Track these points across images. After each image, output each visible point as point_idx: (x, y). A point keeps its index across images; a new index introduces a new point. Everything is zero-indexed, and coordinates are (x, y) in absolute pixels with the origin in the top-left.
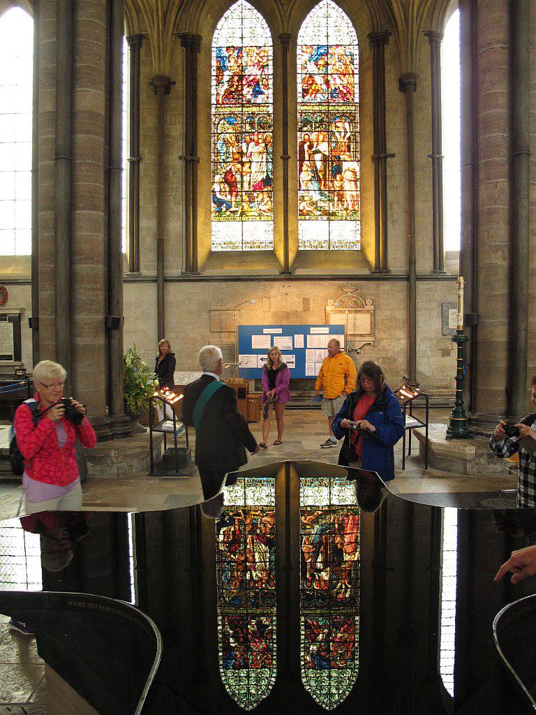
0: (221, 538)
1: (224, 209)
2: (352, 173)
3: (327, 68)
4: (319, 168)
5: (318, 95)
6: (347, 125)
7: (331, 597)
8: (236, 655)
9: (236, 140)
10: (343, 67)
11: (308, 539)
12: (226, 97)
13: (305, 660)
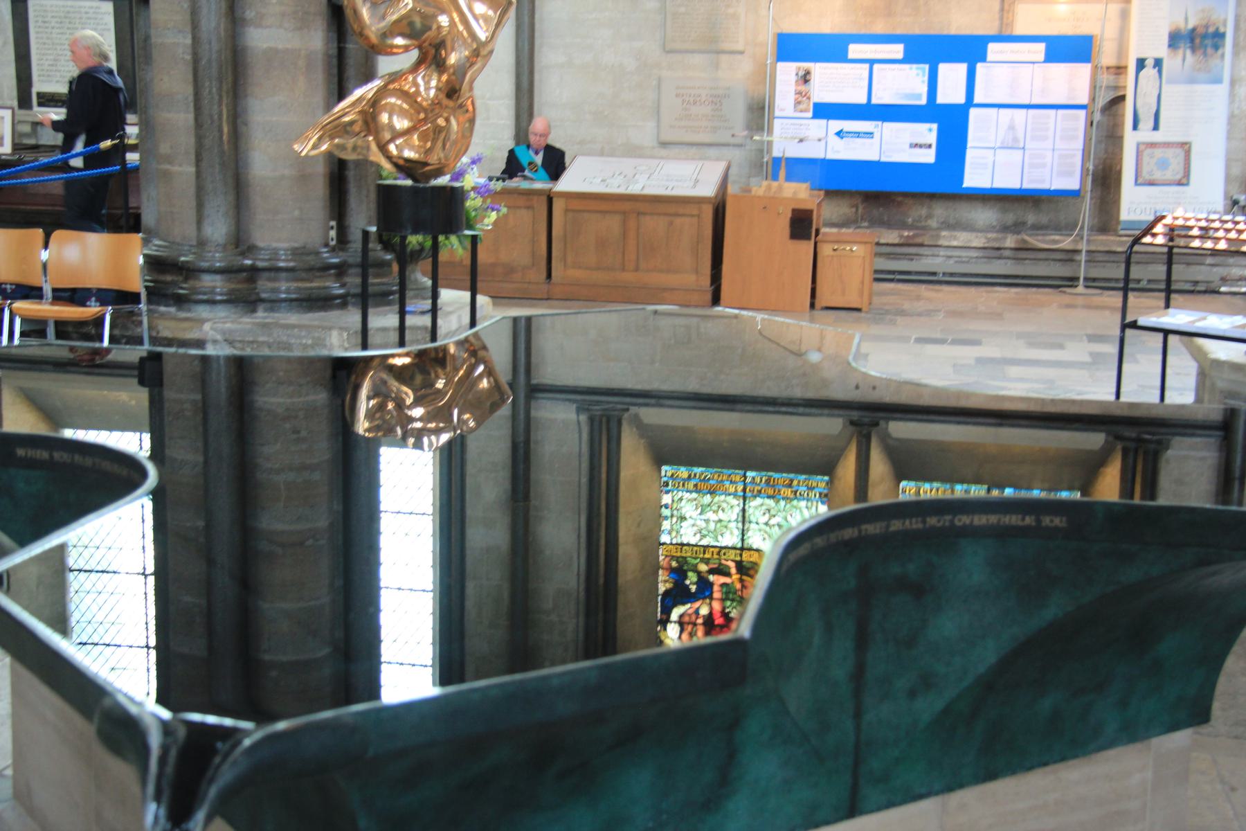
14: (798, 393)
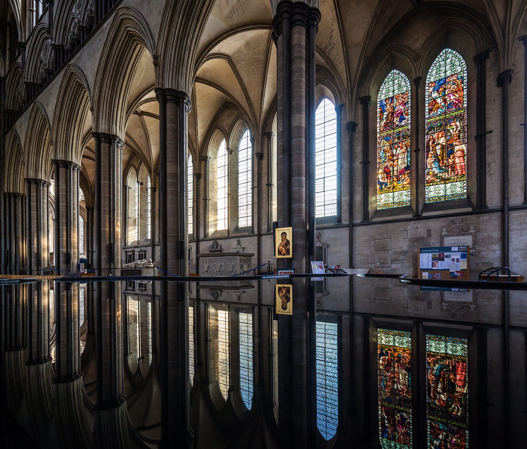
0: (381, 362)
1: (384, 187)
2: (461, 152)
3: (445, 92)
4: (439, 153)
5: (440, 110)
6: (458, 123)
7: (448, 412)
8: (388, 431)
9: (390, 149)
10: (456, 87)
11: (432, 372)
12: (385, 127)
14: (403, 315)
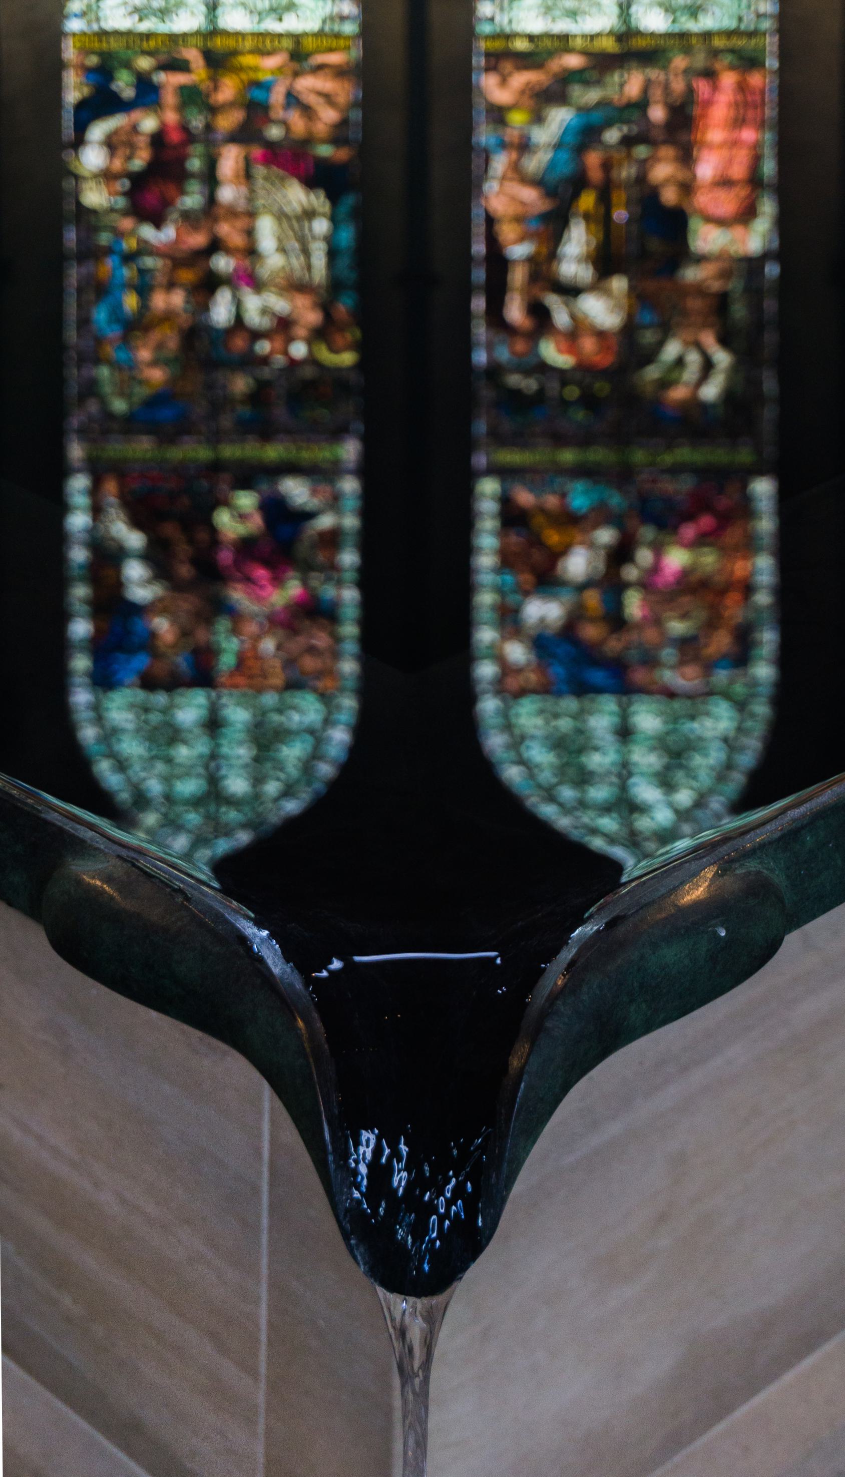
13: (500, 659)
